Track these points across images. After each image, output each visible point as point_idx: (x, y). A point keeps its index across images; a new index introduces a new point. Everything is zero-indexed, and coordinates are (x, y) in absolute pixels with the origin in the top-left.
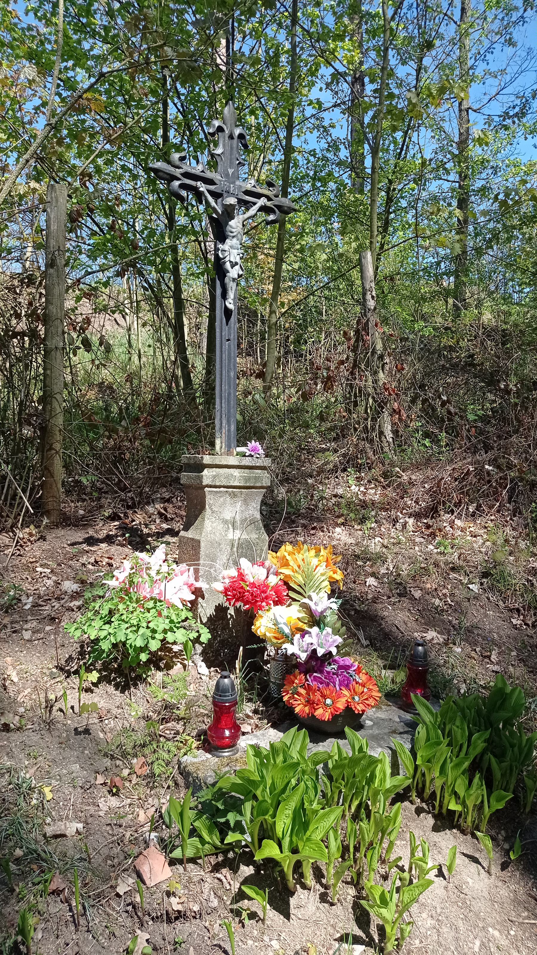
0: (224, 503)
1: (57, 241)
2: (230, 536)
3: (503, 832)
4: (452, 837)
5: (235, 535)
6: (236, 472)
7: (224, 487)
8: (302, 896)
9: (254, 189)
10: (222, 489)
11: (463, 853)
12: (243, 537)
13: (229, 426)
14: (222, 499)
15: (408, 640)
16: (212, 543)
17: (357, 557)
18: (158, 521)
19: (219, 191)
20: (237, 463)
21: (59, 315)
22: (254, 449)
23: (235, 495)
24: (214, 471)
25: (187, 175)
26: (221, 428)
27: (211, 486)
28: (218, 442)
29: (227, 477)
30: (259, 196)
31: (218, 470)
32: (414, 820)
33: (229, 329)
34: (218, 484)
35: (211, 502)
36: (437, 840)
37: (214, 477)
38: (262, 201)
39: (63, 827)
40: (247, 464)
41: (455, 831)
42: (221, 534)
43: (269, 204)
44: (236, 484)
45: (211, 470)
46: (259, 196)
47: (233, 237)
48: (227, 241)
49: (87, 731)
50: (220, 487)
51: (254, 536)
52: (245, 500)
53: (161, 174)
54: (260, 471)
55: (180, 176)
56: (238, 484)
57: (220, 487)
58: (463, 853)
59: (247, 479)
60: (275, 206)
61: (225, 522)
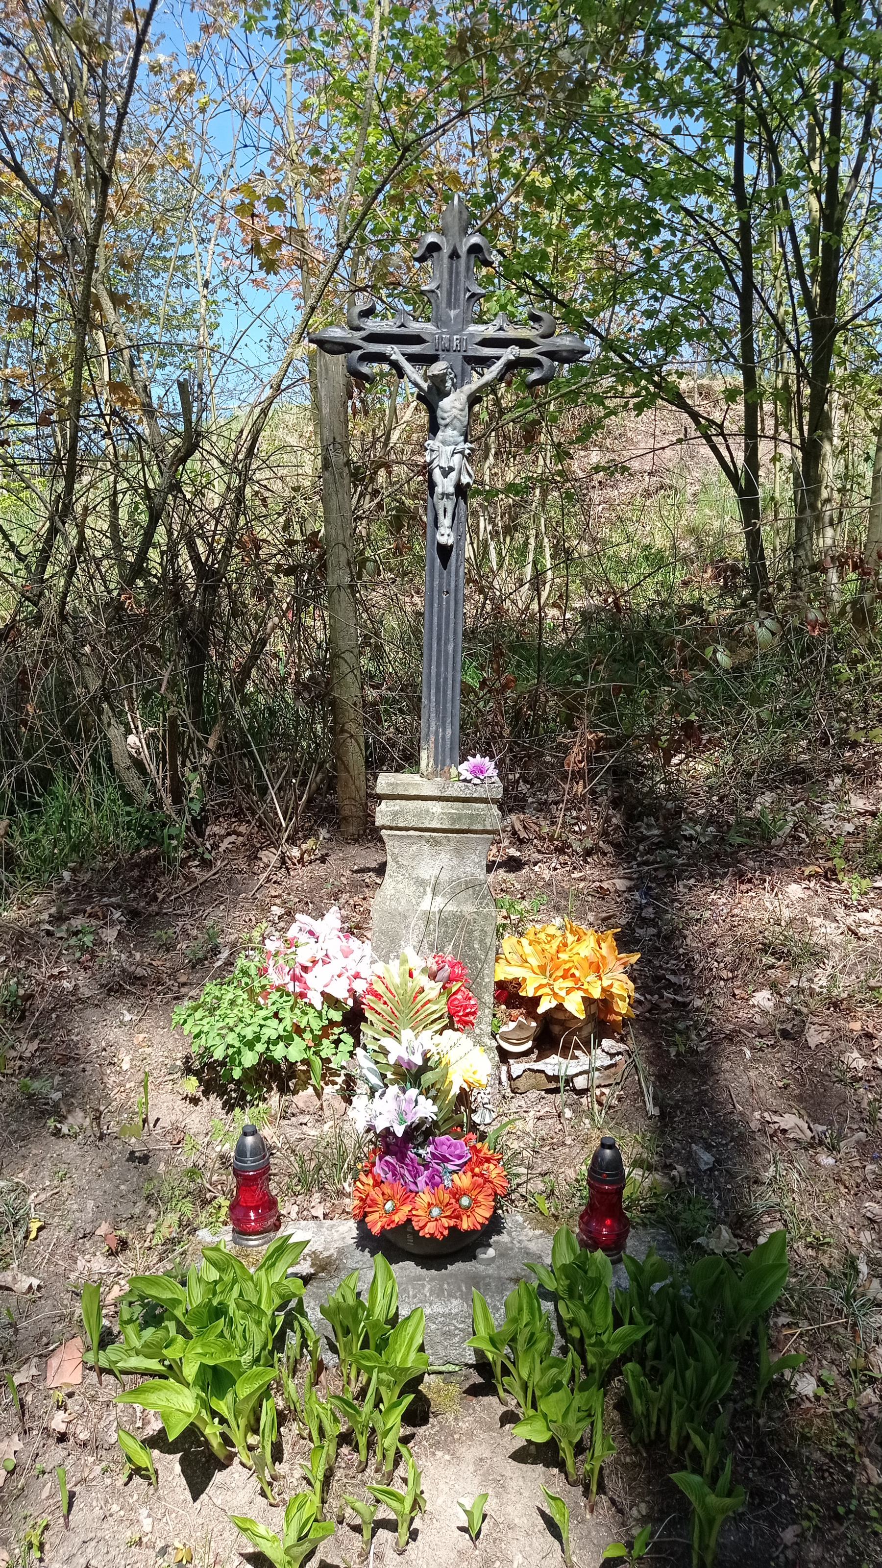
0: (420, 853)
1: (331, 430)
2: (425, 905)
3: (643, 1506)
4: (542, 1480)
5: (437, 904)
6: (437, 808)
7: (416, 829)
8: (236, 1475)
9: (502, 335)
10: (411, 833)
11: (543, 1514)
12: (449, 908)
13: (444, 731)
14: (414, 847)
15: (733, 1124)
16: (392, 915)
17: (766, 948)
18: (506, 843)
19: (433, 352)
20: (436, 793)
21: (341, 538)
22: (478, 770)
23: (437, 843)
24: (397, 805)
25: (373, 338)
26: (428, 735)
27: (391, 828)
28: (424, 755)
29: (418, 815)
30: (504, 343)
31: (404, 803)
32: (490, 1429)
33: (449, 573)
34: (401, 825)
35: (396, 851)
36: (508, 1474)
37: (395, 814)
38: (510, 353)
39: (10, 1279)
40: (455, 794)
41: (555, 1471)
42: (409, 901)
43: (526, 353)
44: (435, 825)
45: (392, 803)
46: (504, 343)
47: (446, 426)
48: (440, 433)
49: (145, 1159)
50: (407, 829)
51: (469, 909)
52: (457, 851)
53: (327, 346)
54: (483, 806)
55: (360, 343)
56: (439, 826)
57: (407, 829)
58: (543, 1514)
59: (453, 818)
60: (541, 354)
61: (421, 883)
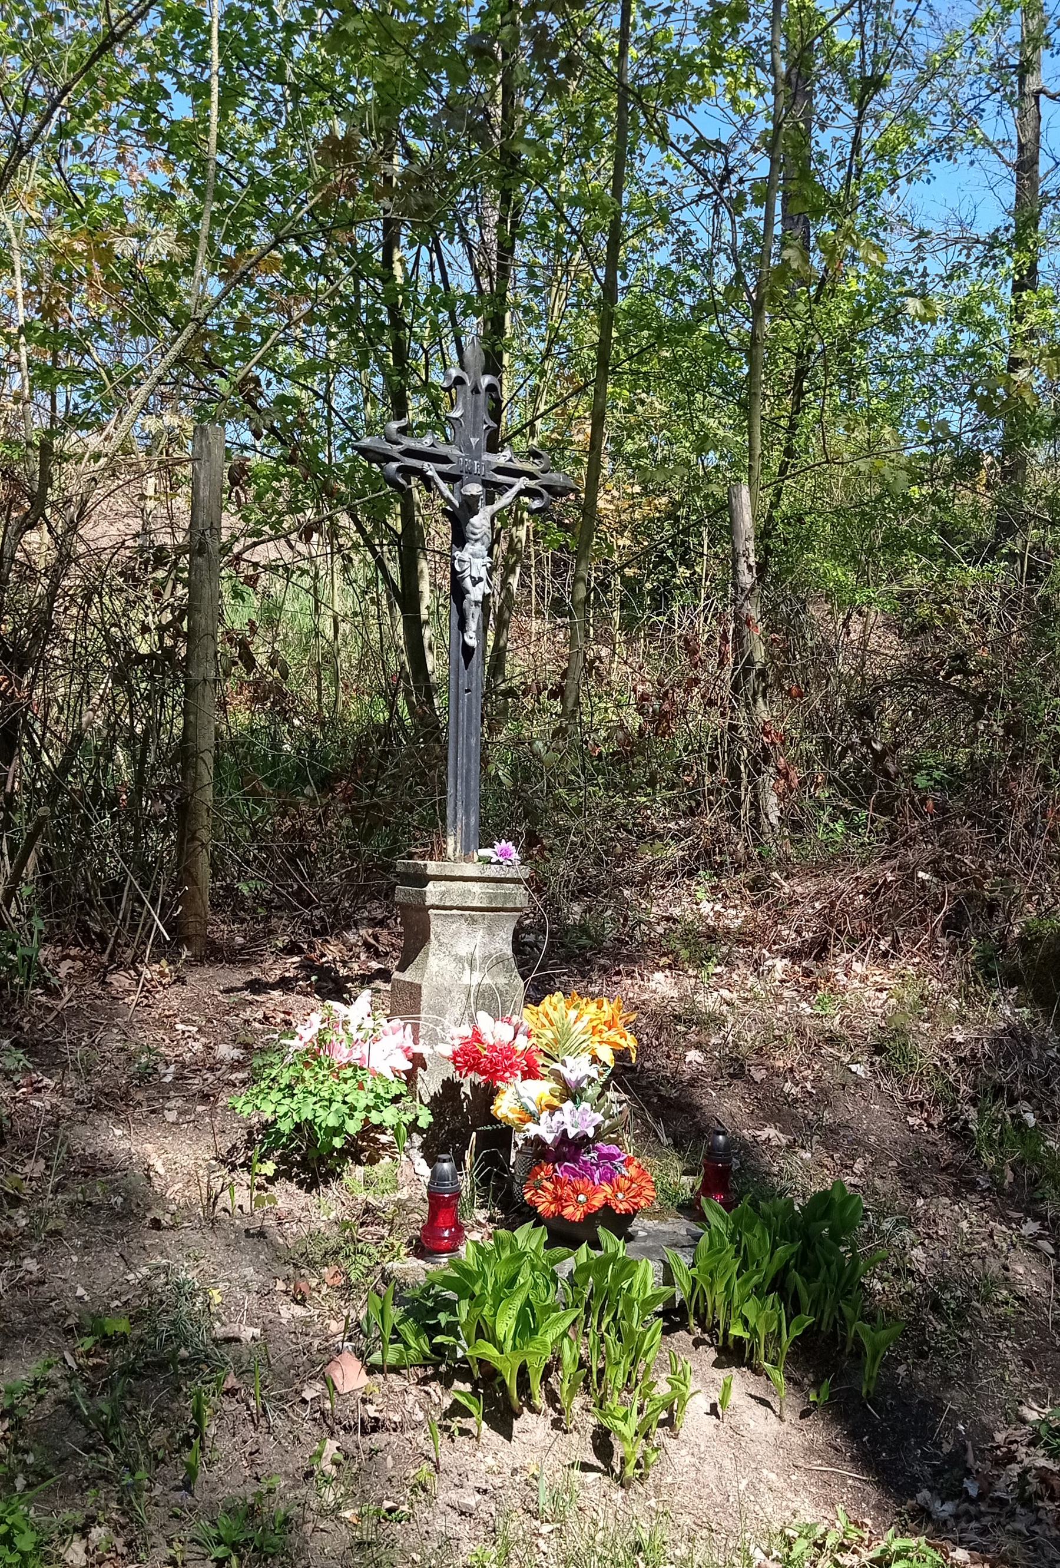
1: (209, 515)
2: (466, 979)
3: (811, 1376)
6: (476, 887)
7: (458, 908)
9: (510, 465)
10: (454, 912)
11: (751, 1396)
12: (485, 982)
13: (468, 818)
14: (454, 926)
16: (438, 991)
20: (477, 874)
22: (504, 853)
23: (474, 921)
24: (443, 886)
26: (455, 822)
27: (438, 908)
28: (451, 841)
29: (463, 894)
30: (518, 474)
31: (448, 883)
33: (470, 673)
34: (448, 904)
37: (443, 894)
38: (522, 483)
43: (532, 484)
44: (476, 904)
45: (438, 884)
46: (518, 474)
47: (476, 541)
50: (451, 908)
51: (502, 981)
54: (512, 886)
57: (451, 908)
58: (751, 1396)
59: (492, 897)
61: (459, 959)
